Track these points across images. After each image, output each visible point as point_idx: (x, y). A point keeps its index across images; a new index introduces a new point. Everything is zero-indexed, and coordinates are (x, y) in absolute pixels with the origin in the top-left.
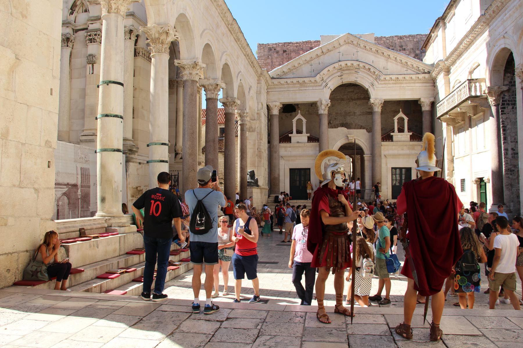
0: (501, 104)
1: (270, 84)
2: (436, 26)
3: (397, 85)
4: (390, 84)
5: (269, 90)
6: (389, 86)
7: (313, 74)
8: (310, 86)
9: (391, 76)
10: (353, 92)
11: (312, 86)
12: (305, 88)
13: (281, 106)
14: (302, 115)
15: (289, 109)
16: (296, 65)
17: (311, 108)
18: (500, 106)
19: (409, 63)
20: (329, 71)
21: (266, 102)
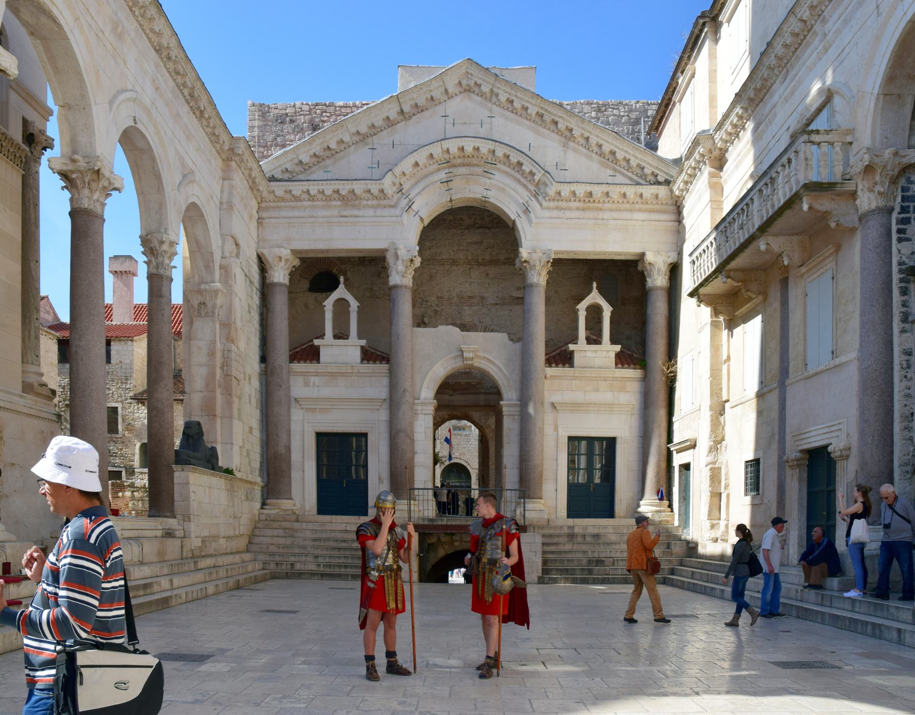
0: (897, 209)
1: (265, 194)
2: (692, 49)
3: (588, 214)
4: (570, 209)
5: (264, 215)
6: (568, 214)
7: (377, 173)
9: (574, 187)
10: (481, 242)
11: (373, 207)
12: (356, 212)
13: (297, 262)
14: (348, 287)
15: (320, 273)
16: (333, 145)
17: (373, 265)
18: (895, 215)
19: (620, 155)
21: (254, 245)
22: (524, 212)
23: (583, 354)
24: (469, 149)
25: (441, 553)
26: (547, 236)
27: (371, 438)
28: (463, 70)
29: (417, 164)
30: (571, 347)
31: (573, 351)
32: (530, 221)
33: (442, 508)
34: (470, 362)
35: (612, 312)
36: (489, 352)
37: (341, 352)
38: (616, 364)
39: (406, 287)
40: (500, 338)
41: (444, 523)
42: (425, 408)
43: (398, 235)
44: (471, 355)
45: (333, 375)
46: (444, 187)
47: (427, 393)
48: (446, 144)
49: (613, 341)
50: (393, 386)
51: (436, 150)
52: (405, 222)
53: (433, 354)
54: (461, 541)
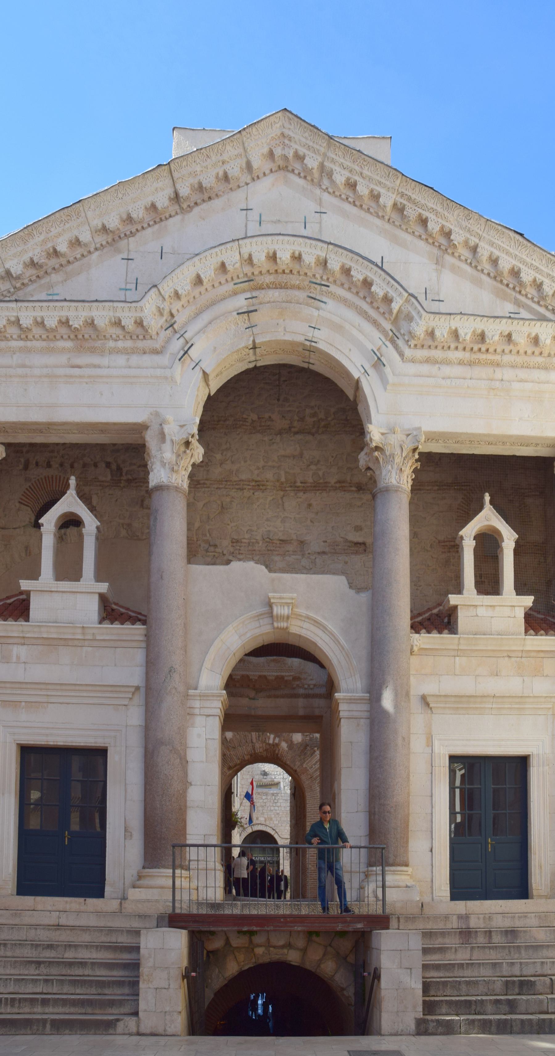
8: (118, 351)
20: (198, 281)
22: (375, 366)
23: (472, 612)
24: (284, 256)
25: (232, 968)
26: (415, 408)
27: (113, 759)
28: (276, 131)
29: (198, 281)
30: (454, 599)
31: (455, 608)
32: (384, 381)
33: (233, 883)
34: (283, 625)
35: (517, 542)
36: (314, 605)
37: (65, 602)
38: (526, 631)
39: (177, 488)
40: (334, 583)
41: (237, 911)
42: (208, 704)
43: (165, 400)
44: (285, 611)
45: (53, 644)
46: (242, 321)
47: (211, 678)
48: (248, 247)
49: (520, 589)
50: (152, 663)
51: (232, 257)
52: (178, 378)
53: (221, 612)
54: (268, 945)
